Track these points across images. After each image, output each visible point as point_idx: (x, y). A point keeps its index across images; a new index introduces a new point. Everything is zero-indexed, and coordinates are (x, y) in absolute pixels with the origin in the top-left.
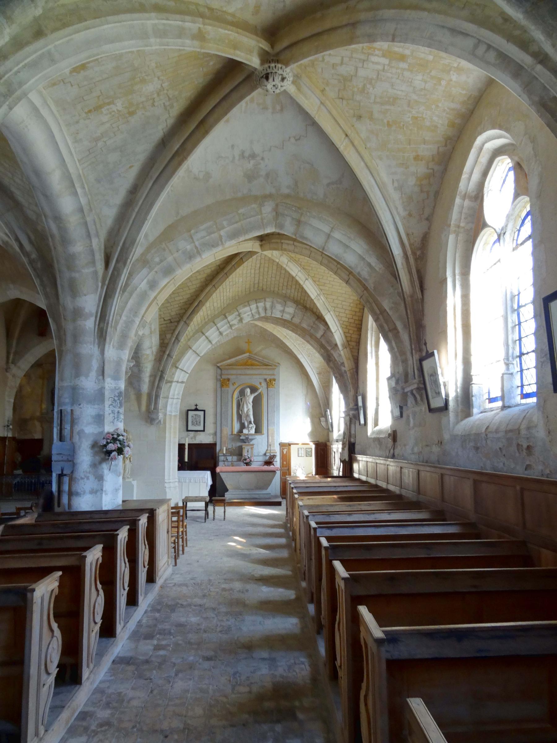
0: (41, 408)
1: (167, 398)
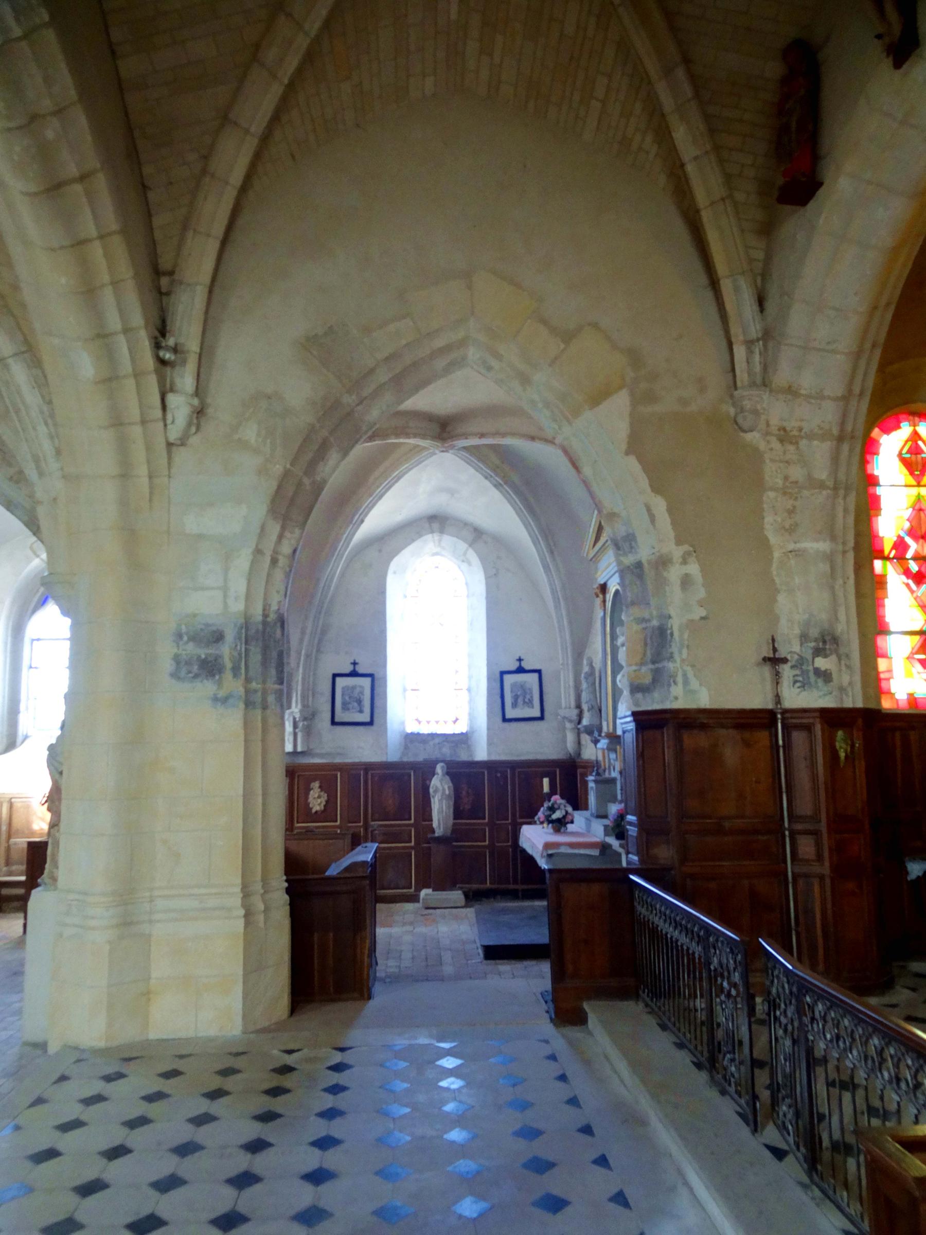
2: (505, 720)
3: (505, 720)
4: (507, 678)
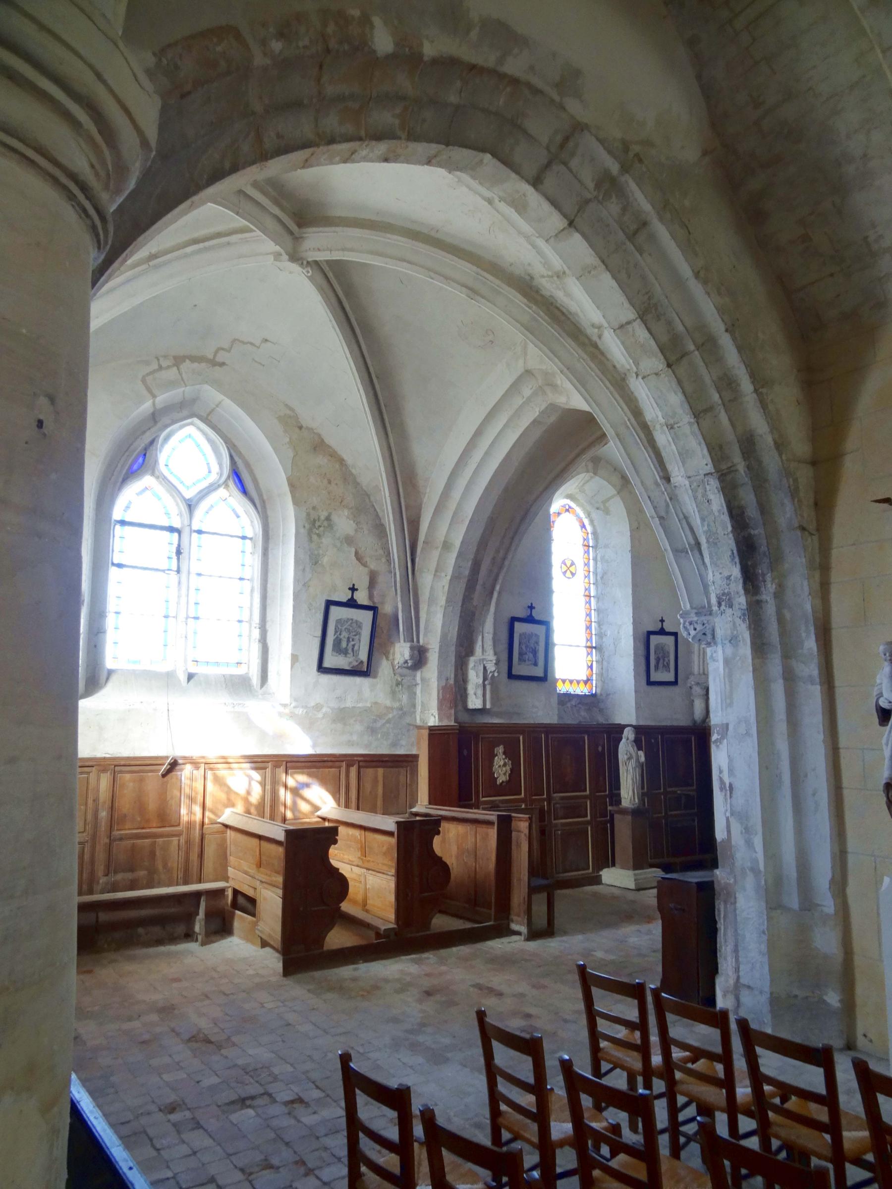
2: (650, 683)
4: (652, 637)
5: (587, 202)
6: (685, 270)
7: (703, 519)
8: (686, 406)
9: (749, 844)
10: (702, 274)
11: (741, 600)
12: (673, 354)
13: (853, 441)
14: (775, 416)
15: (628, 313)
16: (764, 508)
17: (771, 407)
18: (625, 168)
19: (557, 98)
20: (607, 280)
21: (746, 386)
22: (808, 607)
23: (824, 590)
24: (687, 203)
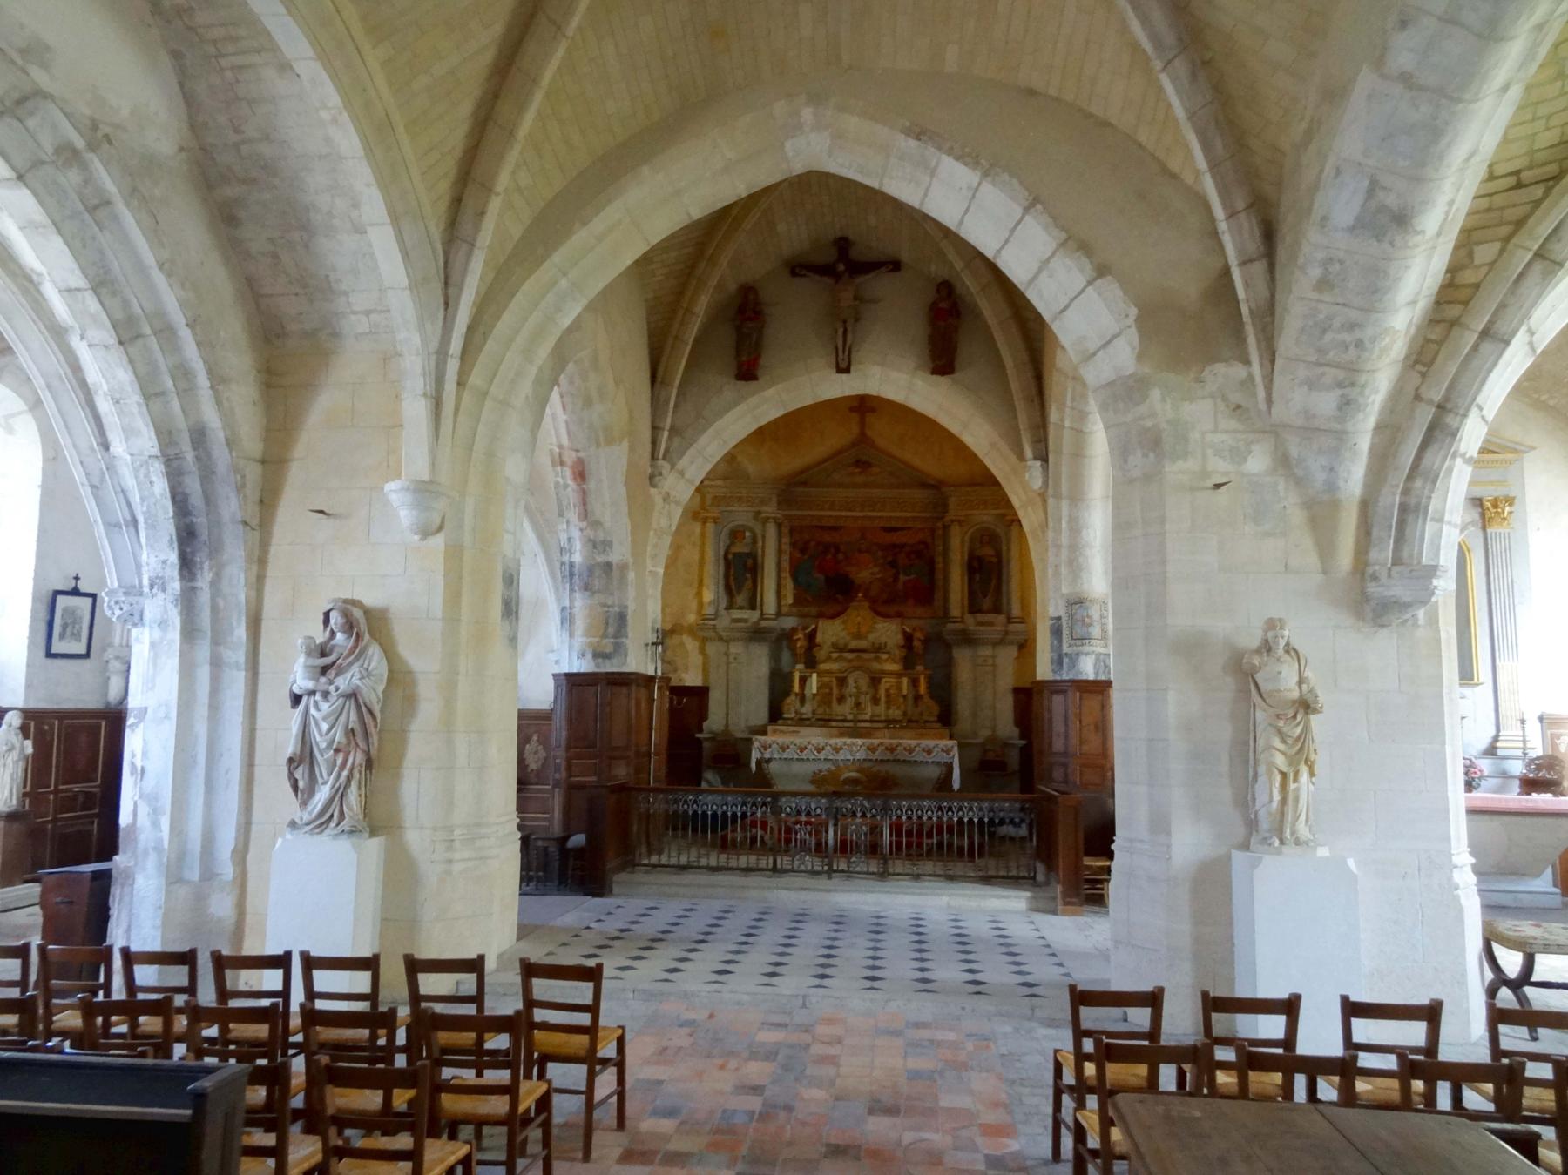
0: (701, 604)
1: (1440, 520)
2: (49, 655)
3: (49, 655)
4: (60, 599)
5: (43, 163)
6: (150, 259)
7: (143, 499)
8: (136, 386)
9: (156, 825)
10: (166, 266)
11: (176, 586)
12: (126, 333)
13: (299, 450)
14: (230, 413)
15: (77, 280)
16: (208, 498)
17: (226, 404)
18: (92, 147)
19: (19, 61)
20: (57, 243)
21: (203, 380)
22: (242, 597)
23: (259, 583)
24: (157, 192)
